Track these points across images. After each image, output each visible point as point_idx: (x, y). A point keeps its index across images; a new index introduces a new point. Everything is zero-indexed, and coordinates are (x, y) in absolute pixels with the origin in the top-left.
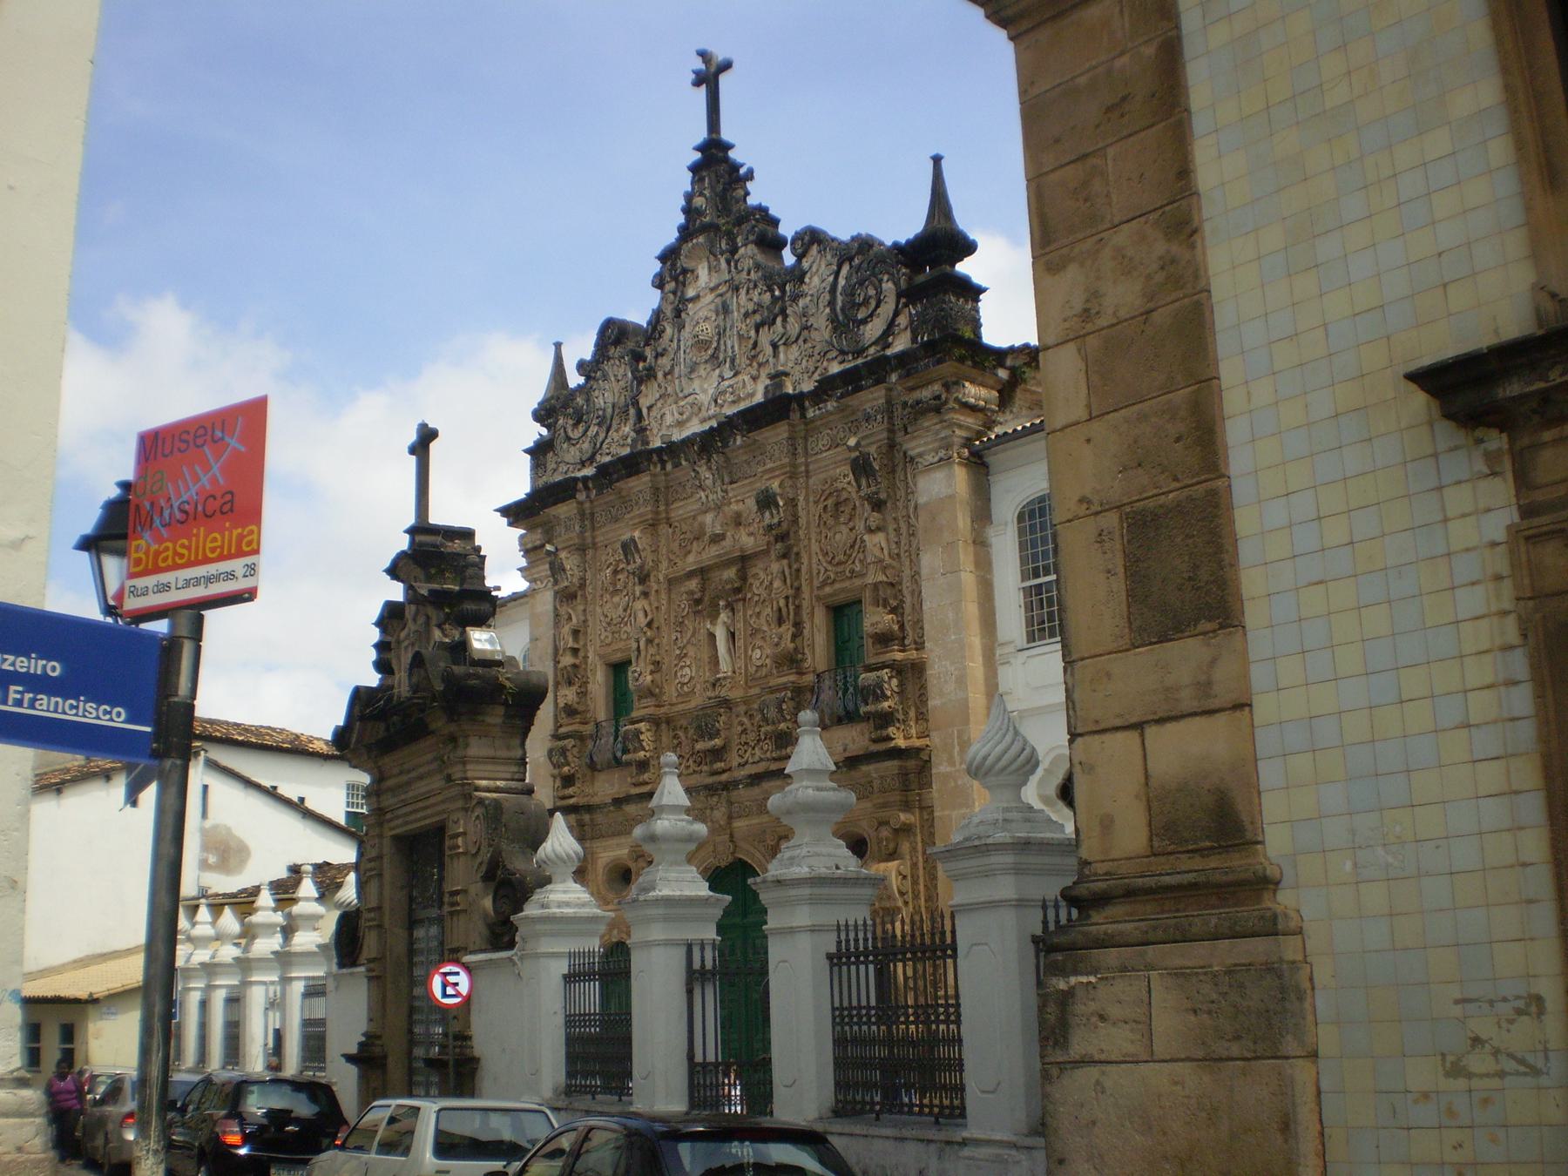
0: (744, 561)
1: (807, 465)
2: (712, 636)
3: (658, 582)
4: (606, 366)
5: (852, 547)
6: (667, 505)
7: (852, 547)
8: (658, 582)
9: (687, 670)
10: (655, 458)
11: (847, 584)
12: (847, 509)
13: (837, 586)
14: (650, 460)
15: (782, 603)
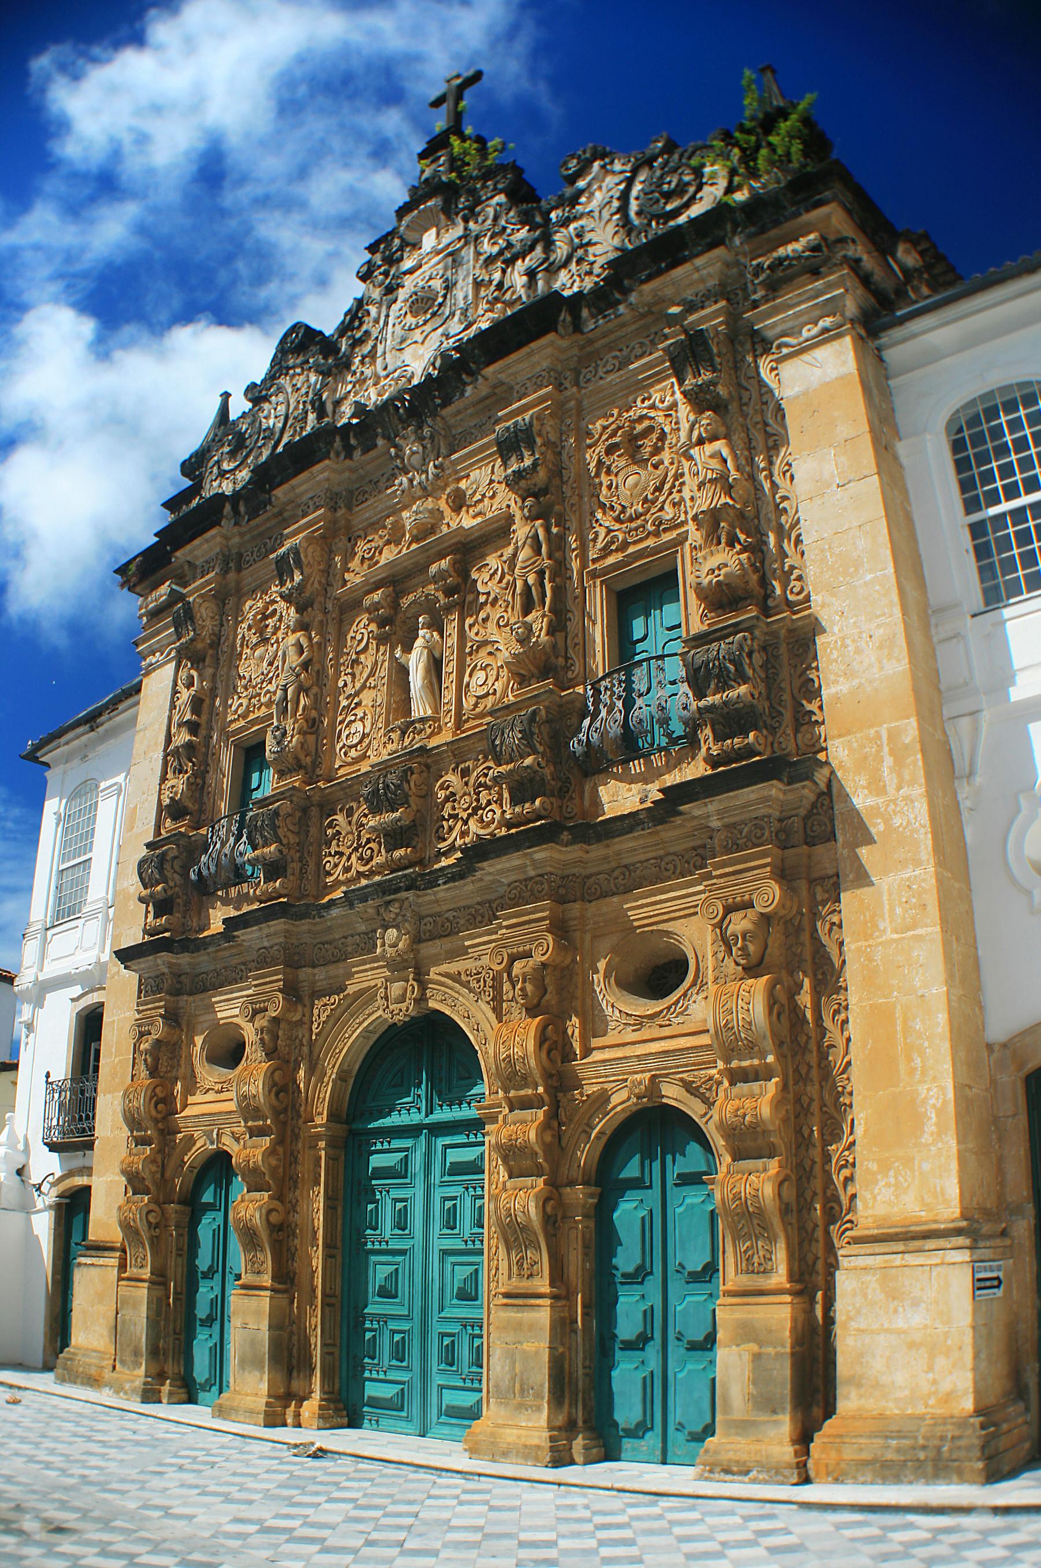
0: (469, 550)
1: (579, 403)
2: (403, 671)
3: (325, 612)
4: (284, 381)
5: (659, 489)
6: (349, 508)
7: (659, 489)
8: (325, 612)
9: (359, 725)
10: (338, 443)
11: (650, 542)
12: (648, 443)
13: (631, 550)
14: (331, 443)
15: (531, 579)
